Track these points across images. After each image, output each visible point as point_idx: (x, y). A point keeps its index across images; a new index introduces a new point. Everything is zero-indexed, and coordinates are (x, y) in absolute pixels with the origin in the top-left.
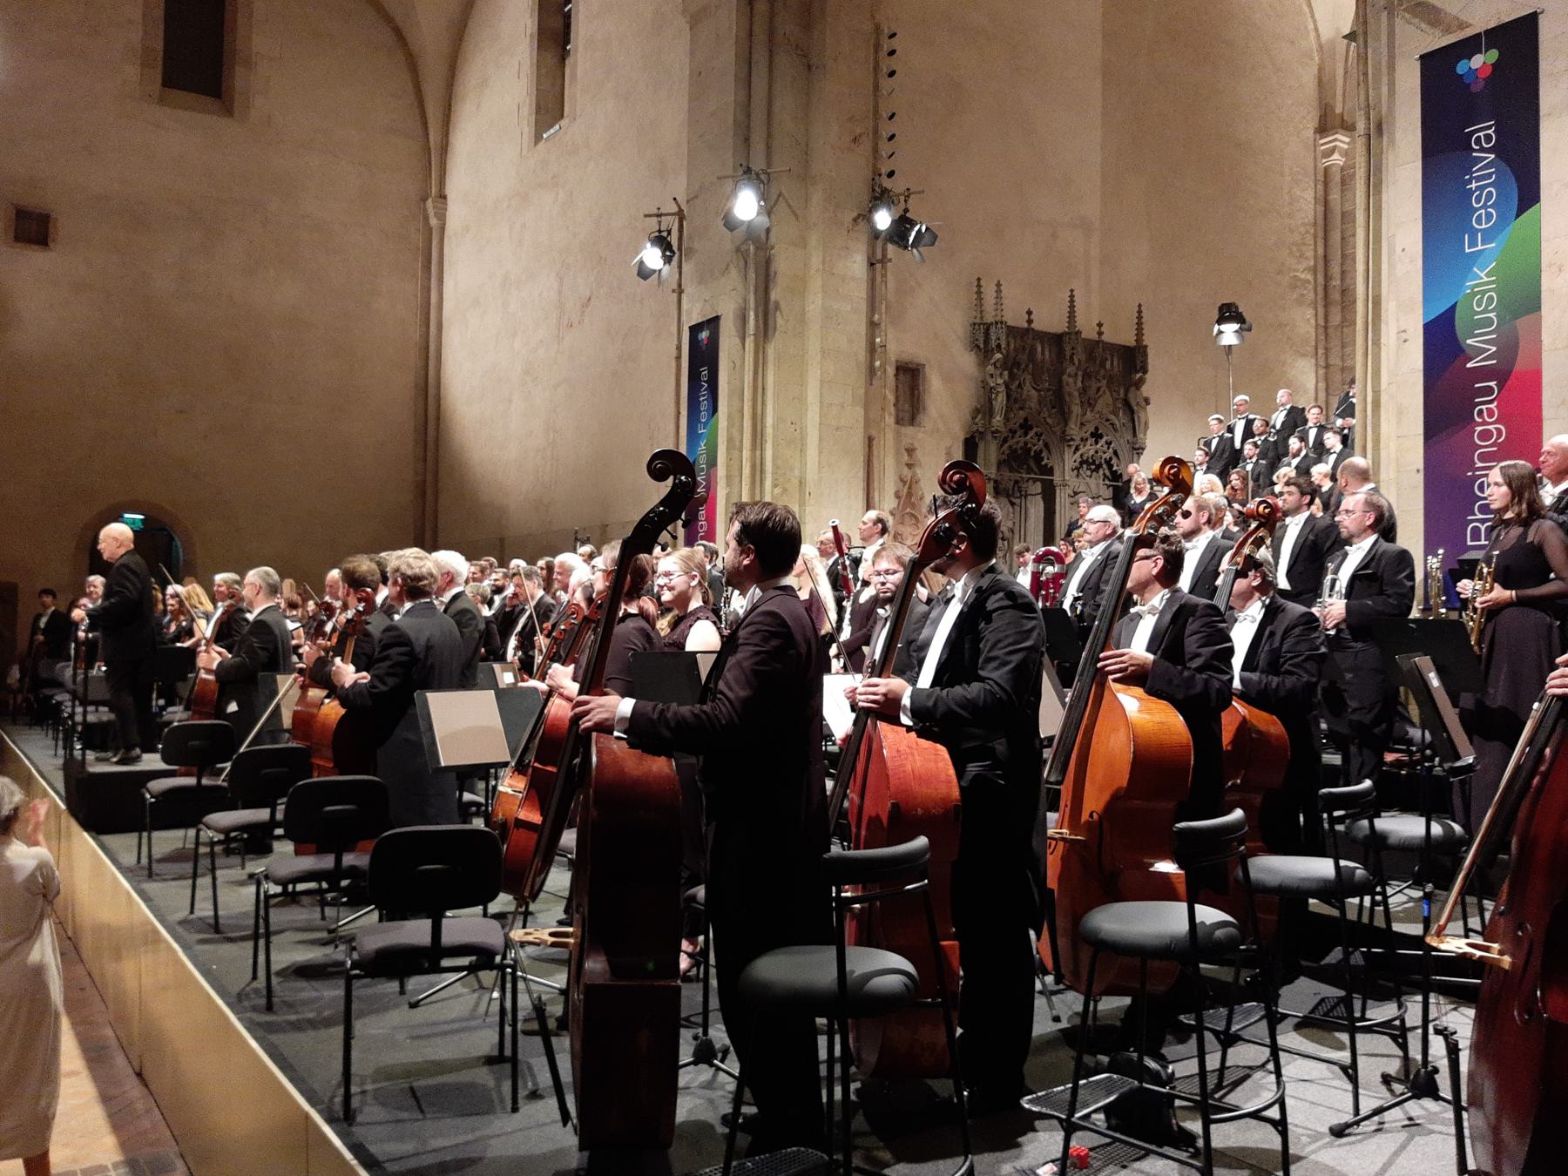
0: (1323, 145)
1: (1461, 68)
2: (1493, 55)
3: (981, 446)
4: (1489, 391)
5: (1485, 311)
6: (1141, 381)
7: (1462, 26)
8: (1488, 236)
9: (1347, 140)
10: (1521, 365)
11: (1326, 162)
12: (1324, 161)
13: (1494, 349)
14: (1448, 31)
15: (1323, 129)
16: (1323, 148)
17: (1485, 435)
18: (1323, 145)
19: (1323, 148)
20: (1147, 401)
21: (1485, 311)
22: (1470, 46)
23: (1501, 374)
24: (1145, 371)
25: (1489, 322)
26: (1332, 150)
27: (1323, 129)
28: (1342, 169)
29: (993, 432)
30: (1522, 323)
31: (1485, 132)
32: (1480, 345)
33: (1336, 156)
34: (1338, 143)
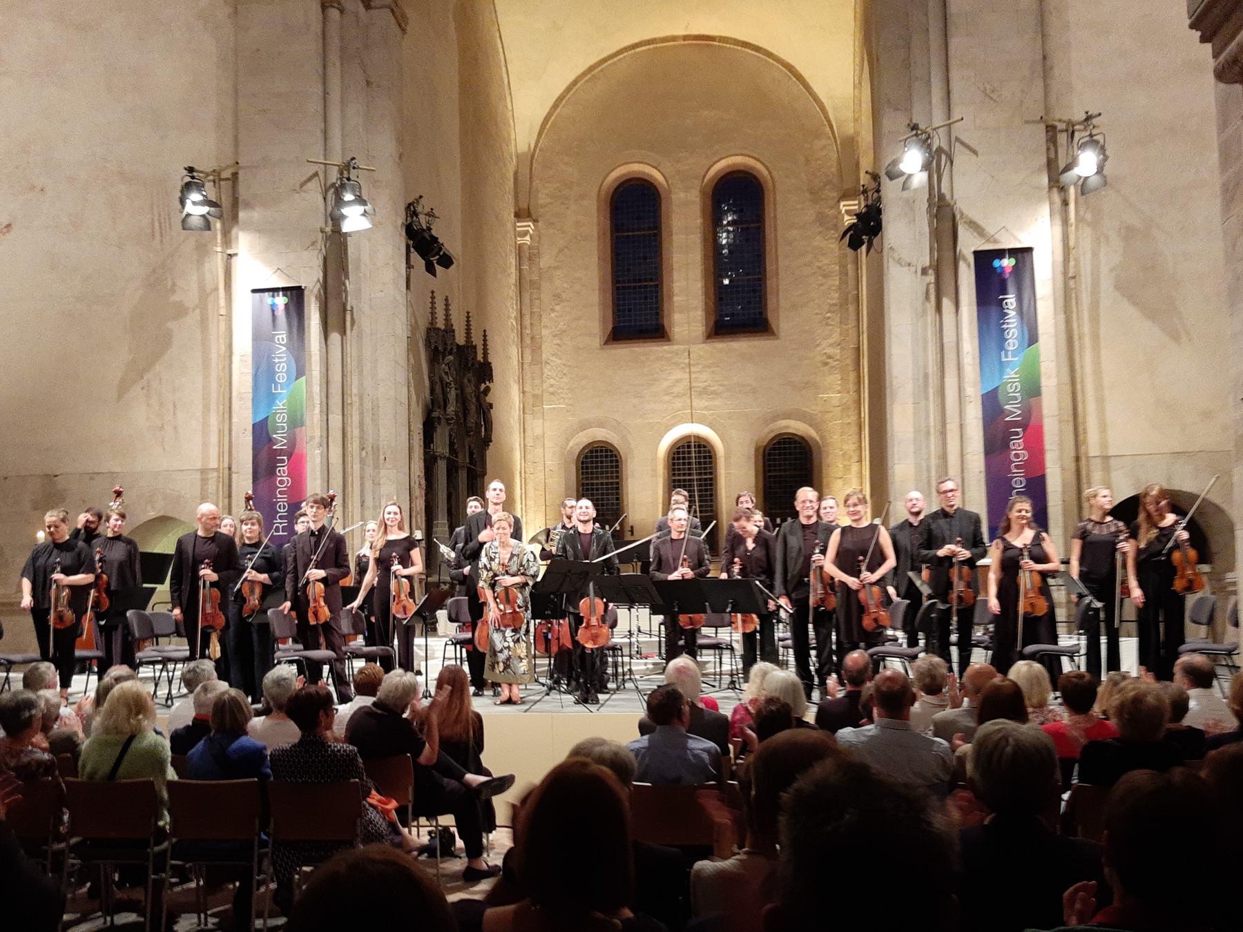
0: (519, 227)
1: (996, 263)
2: (1012, 262)
3: (439, 430)
4: (1017, 433)
5: (1013, 392)
6: (488, 390)
7: (996, 241)
8: (1015, 354)
9: (533, 227)
10: (1033, 421)
11: (520, 240)
12: (519, 239)
13: (1019, 412)
14: (988, 241)
15: (518, 215)
16: (518, 229)
17: (1017, 456)
18: (519, 227)
19: (518, 229)
20: (491, 406)
21: (1013, 392)
22: (1000, 254)
23: (1024, 425)
24: (491, 379)
25: (1016, 398)
26: (525, 234)
27: (518, 215)
28: (530, 248)
29: (447, 419)
30: (1033, 400)
31: (1011, 300)
32: (1013, 409)
33: (528, 238)
34: (529, 229)
